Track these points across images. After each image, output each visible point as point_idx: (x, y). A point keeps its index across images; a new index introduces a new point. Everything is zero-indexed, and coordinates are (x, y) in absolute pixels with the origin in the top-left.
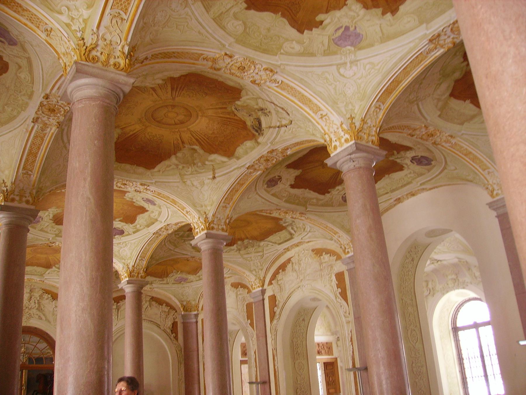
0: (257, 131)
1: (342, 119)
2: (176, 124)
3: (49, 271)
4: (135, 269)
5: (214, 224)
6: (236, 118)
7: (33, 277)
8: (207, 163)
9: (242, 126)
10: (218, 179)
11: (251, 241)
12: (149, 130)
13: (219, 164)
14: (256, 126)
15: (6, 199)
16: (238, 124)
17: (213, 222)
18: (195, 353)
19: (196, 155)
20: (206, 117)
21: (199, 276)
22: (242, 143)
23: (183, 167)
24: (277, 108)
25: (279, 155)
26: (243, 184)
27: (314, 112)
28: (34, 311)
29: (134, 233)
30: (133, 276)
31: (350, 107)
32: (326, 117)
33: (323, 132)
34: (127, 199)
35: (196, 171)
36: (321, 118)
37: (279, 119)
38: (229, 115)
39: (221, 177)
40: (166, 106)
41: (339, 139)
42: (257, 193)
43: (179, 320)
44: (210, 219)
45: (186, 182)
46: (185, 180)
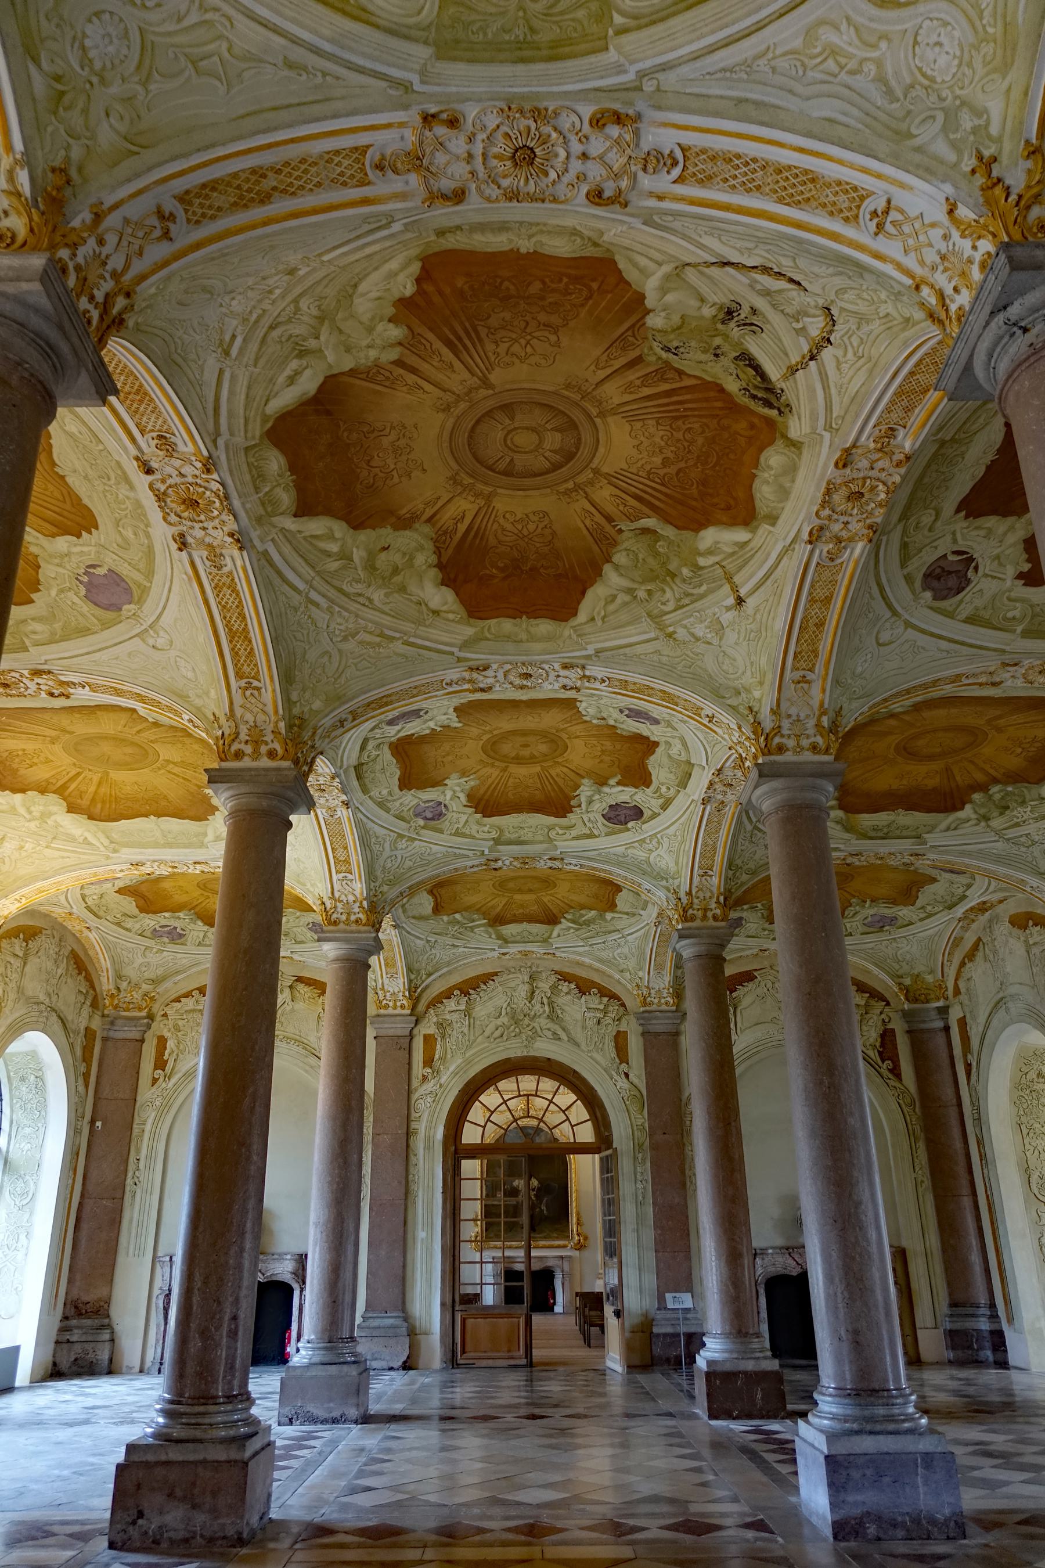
0: (768, 404)
1: (948, 189)
2: (556, 467)
3: (557, 930)
4: (696, 901)
5: (782, 736)
7: (529, 947)
8: (702, 561)
9: (719, 404)
10: (751, 603)
11: (1010, 789)
12: (500, 504)
13: (733, 554)
14: (756, 387)
15: (223, 756)
16: (707, 400)
17: (778, 730)
18: (953, 1112)
19: (661, 547)
20: (614, 412)
21: (923, 908)
22: (756, 465)
23: (650, 592)
24: (756, 281)
25: (880, 465)
26: (828, 600)
27: (846, 220)
28: (543, 1022)
29: (664, 807)
30: (693, 919)
31: (967, 122)
32: (894, 215)
33: (909, 282)
34: (595, 721)
35: (687, 595)
36: (880, 227)
37: (795, 325)
38: (666, 380)
40: (489, 414)
41: (963, 274)
42: (908, 625)
43: (898, 1026)
44: (768, 724)
45: (675, 632)
46: (671, 629)
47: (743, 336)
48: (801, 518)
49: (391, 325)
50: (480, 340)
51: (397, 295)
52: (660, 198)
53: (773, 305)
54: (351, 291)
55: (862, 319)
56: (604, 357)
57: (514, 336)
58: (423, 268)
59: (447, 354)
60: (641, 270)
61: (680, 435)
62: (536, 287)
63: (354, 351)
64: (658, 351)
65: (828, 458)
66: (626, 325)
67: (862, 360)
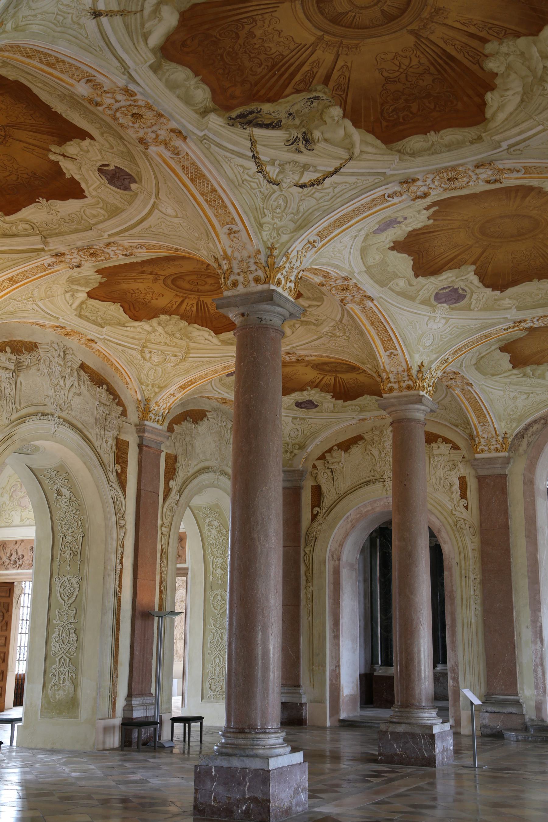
0: (241, 116)
6: (289, 90)
9: (262, 92)
10: (91, 24)
13: (143, 25)
14: (256, 118)
20: (314, 45)
22: (203, 81)
24: (316, 171)
38: (301, 81)
39: (97, 30)
47: (290, 134)
48: (147, 89)
49: (495, 71)
50: (432, 64)
51: (495, 92)
52: (386, 189)
53: (296, 162)
54: (525, 97)
55: (266, 198)
56: (347, 74)
57: (411, 70)
58: (484, 113)
59: (450, 50)
60: (367, 143)
61: (262, 57)
62: (414, 107)
63: (518, 53)
64: (320, 95)
65: (184, 126)
66: (349, 101)
67: (241, 182)
